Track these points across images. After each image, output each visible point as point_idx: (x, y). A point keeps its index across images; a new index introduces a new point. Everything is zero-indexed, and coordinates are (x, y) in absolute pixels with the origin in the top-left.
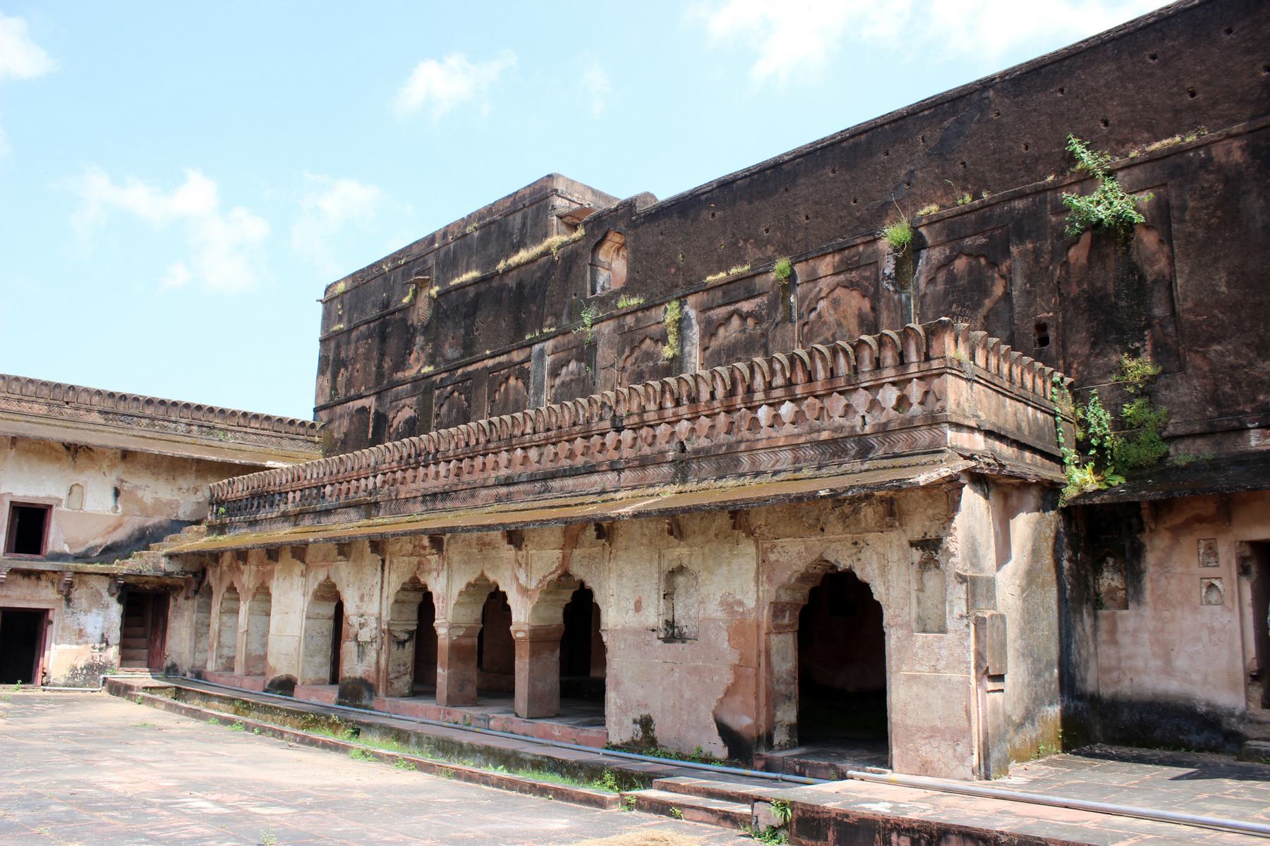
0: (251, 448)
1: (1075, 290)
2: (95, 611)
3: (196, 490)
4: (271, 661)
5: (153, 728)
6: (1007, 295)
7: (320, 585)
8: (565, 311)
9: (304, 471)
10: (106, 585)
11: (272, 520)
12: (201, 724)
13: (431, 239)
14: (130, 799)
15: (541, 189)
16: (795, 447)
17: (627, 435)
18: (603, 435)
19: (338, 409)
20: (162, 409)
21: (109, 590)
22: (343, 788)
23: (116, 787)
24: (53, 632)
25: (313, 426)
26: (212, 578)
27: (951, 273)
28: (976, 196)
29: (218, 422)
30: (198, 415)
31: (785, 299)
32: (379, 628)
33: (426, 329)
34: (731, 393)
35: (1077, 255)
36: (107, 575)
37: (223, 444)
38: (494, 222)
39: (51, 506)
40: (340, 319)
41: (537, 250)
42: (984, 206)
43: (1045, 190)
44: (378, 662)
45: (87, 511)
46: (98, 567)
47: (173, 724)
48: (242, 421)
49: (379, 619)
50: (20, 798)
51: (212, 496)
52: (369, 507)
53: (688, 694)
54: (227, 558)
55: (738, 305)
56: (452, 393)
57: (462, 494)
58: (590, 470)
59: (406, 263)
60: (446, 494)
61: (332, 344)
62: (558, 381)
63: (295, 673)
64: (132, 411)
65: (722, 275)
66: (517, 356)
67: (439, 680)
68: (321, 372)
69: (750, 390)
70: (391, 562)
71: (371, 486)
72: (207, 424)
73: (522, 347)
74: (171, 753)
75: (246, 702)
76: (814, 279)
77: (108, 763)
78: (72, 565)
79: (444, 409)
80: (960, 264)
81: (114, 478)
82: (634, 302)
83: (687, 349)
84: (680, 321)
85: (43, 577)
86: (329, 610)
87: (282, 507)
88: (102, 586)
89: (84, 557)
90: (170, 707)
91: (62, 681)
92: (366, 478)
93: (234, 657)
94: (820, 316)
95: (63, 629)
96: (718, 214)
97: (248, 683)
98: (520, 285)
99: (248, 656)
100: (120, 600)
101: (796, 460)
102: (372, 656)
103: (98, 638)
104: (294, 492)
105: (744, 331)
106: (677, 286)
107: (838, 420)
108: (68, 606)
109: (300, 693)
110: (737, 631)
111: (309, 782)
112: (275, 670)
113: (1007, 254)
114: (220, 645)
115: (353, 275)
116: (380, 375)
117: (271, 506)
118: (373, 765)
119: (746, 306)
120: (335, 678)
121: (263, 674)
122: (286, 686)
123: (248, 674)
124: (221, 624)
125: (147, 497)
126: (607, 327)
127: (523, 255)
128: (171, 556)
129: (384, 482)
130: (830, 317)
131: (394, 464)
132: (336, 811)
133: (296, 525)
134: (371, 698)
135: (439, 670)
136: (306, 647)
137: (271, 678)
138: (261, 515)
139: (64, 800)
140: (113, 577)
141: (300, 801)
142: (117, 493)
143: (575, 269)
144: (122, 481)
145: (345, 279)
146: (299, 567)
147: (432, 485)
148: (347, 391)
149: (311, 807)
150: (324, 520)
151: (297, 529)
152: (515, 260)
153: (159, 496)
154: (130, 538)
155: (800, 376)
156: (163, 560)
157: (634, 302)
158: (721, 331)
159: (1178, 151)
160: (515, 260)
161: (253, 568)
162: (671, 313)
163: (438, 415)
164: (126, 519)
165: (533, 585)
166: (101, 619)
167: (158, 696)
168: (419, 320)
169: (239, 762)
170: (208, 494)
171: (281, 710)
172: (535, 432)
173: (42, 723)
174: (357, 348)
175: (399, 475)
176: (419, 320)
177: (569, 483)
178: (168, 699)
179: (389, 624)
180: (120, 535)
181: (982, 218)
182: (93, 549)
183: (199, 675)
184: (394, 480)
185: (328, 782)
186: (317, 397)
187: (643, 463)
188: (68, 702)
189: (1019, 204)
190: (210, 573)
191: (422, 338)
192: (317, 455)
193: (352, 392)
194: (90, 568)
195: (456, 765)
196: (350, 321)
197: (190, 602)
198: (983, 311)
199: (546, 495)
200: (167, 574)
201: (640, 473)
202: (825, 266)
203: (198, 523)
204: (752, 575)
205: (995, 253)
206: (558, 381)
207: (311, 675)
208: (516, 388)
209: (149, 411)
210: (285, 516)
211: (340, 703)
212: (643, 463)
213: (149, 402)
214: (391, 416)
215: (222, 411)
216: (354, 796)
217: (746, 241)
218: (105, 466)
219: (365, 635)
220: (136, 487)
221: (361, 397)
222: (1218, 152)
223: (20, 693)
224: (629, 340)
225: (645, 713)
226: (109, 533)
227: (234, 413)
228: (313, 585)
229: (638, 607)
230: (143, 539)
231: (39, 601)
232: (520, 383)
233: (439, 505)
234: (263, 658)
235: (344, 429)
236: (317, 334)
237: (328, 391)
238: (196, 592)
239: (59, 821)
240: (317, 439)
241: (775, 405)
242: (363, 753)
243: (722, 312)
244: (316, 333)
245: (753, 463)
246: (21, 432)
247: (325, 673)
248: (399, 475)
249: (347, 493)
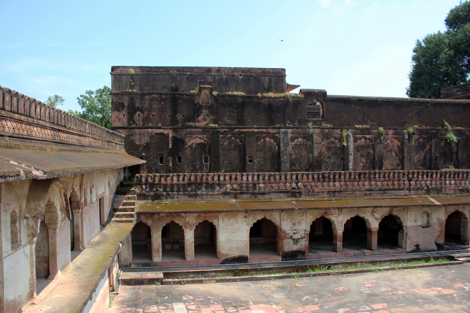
1: (441, 151)
6: (430, 149)
8: (297, 121)
13: (209, 70)
15: (279, 73)
16: (454, 190)
17: (413, 183)
18: (404, 181)
27: (419, 142)
28: (426, 127)
31: (380, 138)
33: (210, 108)
34: (441, 176)
35: (442, 144)
38: (252, 76)
40: (132, 87)
41: (282, 95)
42: (428, 129)
43: (439, 130)
53: (428, 238)
55: (365, 135)
56: (231, 137)
57: (348, 193)
58: (402, 189)
59: (190, 75)
60: (340, 192)
62: (293, 143)
65: (361, 126)
66: (270, 131)
67: (338, 246)
69: (445, 177)
73: (275, 128)
76: (387, 134)
79: (226, 143)
80: (421, 140)
82: (329, 126)
83: (349, 144)
84: (347, 136)
94: (388, 143)
96: (358, 108)
98: (270, 105)
101: (454, 192)
104: (232, 184)
105: (366, 142)
106: (344, 125)
107: (463, 185)
110: (440, 225)
113: (431, 141)
115: (141, 67)
116: (174, 121)
119: (367, 136)
122: (242, 259)
126: (317, 131)
127: (271, 94)
130: (390, 144)
135: (338, 243)
137: (224, 258)
138: (199, 192)
143: (299, 107)
147: (332, 188)
150: (260, 197)
152: (265, 95)
155: (456, 176)
157: (329, 126)
158: (359, 141)
159: (461, 130)
160: (265, 95)
162: (345, 133)
163: (222, 145)
165: (379, 217)
172: (379, 178)
177: (393, 192)
181: (427, 132)
187: (418, 189)
189: (434, 131)
191: (207, 111)
195: (400, 265)
196: (141, 89)
198: (425, 151)
199: (385, 195)
201: (416, 192)
202: (391, 132)
204: (443, 213)
205: (429, 139)
206: (293, 143)
208: (270, 142)
212: (418, 189)
217: (367, 119)
219: (295, 237)
221: (160, 128)
222: (466, 132)
224: (325, 136)
225: (417, 243)
229: (416, 221)
232: (272, 140)
233: (338, 195)
241: (450, 181)
243: (360, 136)
245: (445, 191)
248: (313, 184)
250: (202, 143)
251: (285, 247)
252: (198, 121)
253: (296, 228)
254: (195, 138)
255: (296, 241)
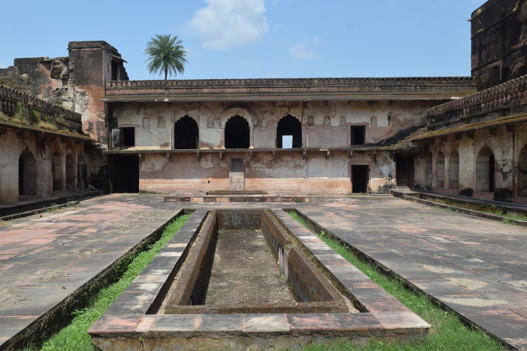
0: (443, 92)
2: (385, 165)
3: (421, 113)
4: (461, 182)
5: (413, 209)
7: (482, 148)
9: (470, 98)
10: (389, 155)
11: (456, 122)
12: (433, 208)
14: (410, 235)
19: (483, 69)
20: (404, 82)
21: (390, 157)
22: (502, 236)
23: (404, 230)
24: (371, 173)
25: (471, 79)
26: (431, 150)
29: (428, 84)
30: (419, 82)
32: (513, 166)
36: (389, 151)
37: (431, 93)
39: (365, 126)
44: (513, 181)
45: (379, 126)
46: (385, 148)
47: (421, 208)
48: (438, 81)
49: (513, 162)
50: (370, 232)
51: (429, 115)
52: (504, 111)
54: (437, 140)
61: (478, 39)
63: (472, 187)
64: (392, 84)
68: (473, 53)
70: (518, 135)
71: (504, 101)
72: (423, 85)
74: (422, 219)
75: (450, 199)
77: (398, 222)
78: (375, 147)
81: (387, 112)
85: (365, 153)
86: (487, 159)
87: (461, 116)
88: (387, 155)
89: (379, 144)
90: (419, 201)
91: (376, 192)
92: (502, 98)
93: (444, 181)
95: (374, 172)
97: (450, 191)
99: (450, 181)
100: (394, 160)
102: (510, 178)
103: (388, 175)
104: (466, 108)
108: (375, 164)
109: (475, 196)
111: (485, 232)
112: (463, 186)
114: (437, 176)
117: (456, 116)
118: (515, 226)
120: (492, 187)
121: (457, 188)
122: (468, 192)
123: (451, 188)
124: (437, 168)
125: (401, 118)
128: (413, 141)
129: (512, 98)
131: (517, 89)
132: (501, 245)
133: (468, 123)
134: (511, 197)
136: (477, 175)
137: (461, 189)
138: (452, 120)
139: (387, 234)
140: (391, 151)
141: (483, 240)
142: (389, 118)
144: (391, 113)
145: (481, 7)
146: (471, 141)
148: (487, 60)
149: (489, 243)
150: (482, 120)
151: (469, 125)
153: (406, 117)
154: (396, 135)
156: (410, 143)
161: (450, 143)
164: (394, 128)
166: (388, 168)
167: (413, 197)
168: (523, 18)
169: (452, 223)
170: (426, 114)
171: (468, 202)
173: (371, 207)
174: (490, 39)
175: (519, 94)
176: (523, 18)
178: (418, 199)
179: (518, 163)
180: (392, 135)
182: (382, 141)
183: (429, 189)
184: (517, 97)
185: (494, 233)
186: (472, 65)
188: (379, 200)
190: (430, 147)
192: (475, 92)
193: (490, 60)
194: (382, 148)
197: (423, 160)
200: (412, 149)
203: (423, 127)
207: (480, 188)
209: (398, 83)
210: (463, 120)
211: (495, 200)
213: (398, 79)
214: (511, 68)
215: (429, 79)
216: (509, 239)
218: (383, 108)
219: (506, 169)
220: (397, 115)
221: (494, 61)
223: (361, 196)
226: (388, 134)
227: (434, 78)
228: (478, 149)
230: (401, 135)
231: (365, 162)
234: (457, 181)
235: (487, 78)
236: (470, 36)
237: (477, 61)
238: (425, 155)
239: (385, 241)
240: (474, 84)
242: (510, 221)
244: (469, 35)
246: (351, 99)
247: (487, 187)
248: (519, 94)
249: (493, 106)
250: (522, 67)
251: (497, 182)
252: (520, 42)
253: (505, 157)
254: (518, 62)
255: (505, 176)
